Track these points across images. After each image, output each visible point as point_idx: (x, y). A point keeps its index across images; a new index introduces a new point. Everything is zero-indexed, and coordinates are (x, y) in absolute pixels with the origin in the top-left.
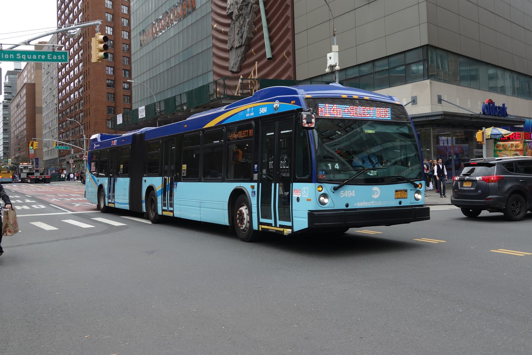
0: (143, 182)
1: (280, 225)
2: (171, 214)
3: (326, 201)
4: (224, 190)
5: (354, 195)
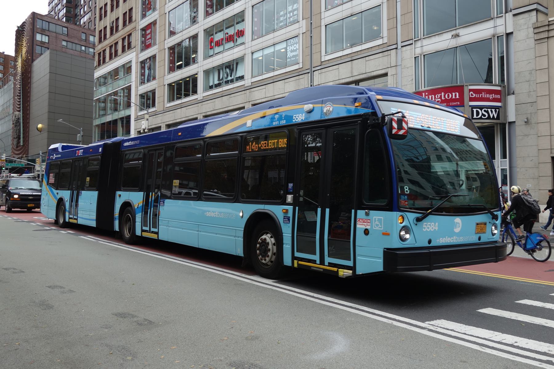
0: (117, 197)
1: (329, 263)
2: (154, 236)
3: (407, 236)
4: (241, 212)
5: (437, 228)
